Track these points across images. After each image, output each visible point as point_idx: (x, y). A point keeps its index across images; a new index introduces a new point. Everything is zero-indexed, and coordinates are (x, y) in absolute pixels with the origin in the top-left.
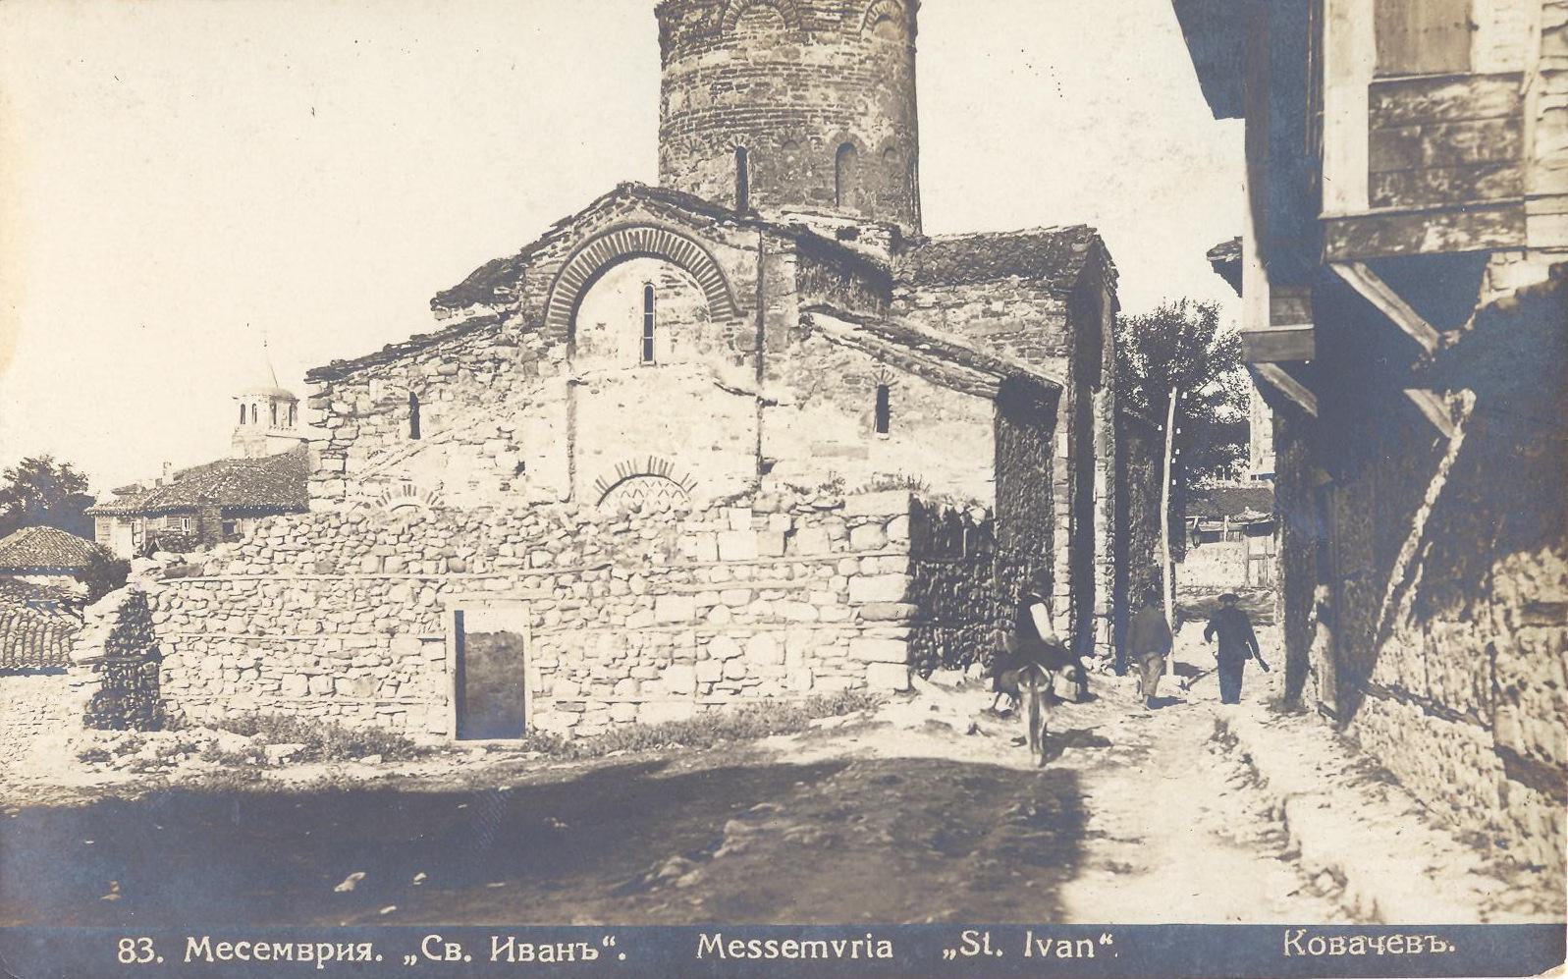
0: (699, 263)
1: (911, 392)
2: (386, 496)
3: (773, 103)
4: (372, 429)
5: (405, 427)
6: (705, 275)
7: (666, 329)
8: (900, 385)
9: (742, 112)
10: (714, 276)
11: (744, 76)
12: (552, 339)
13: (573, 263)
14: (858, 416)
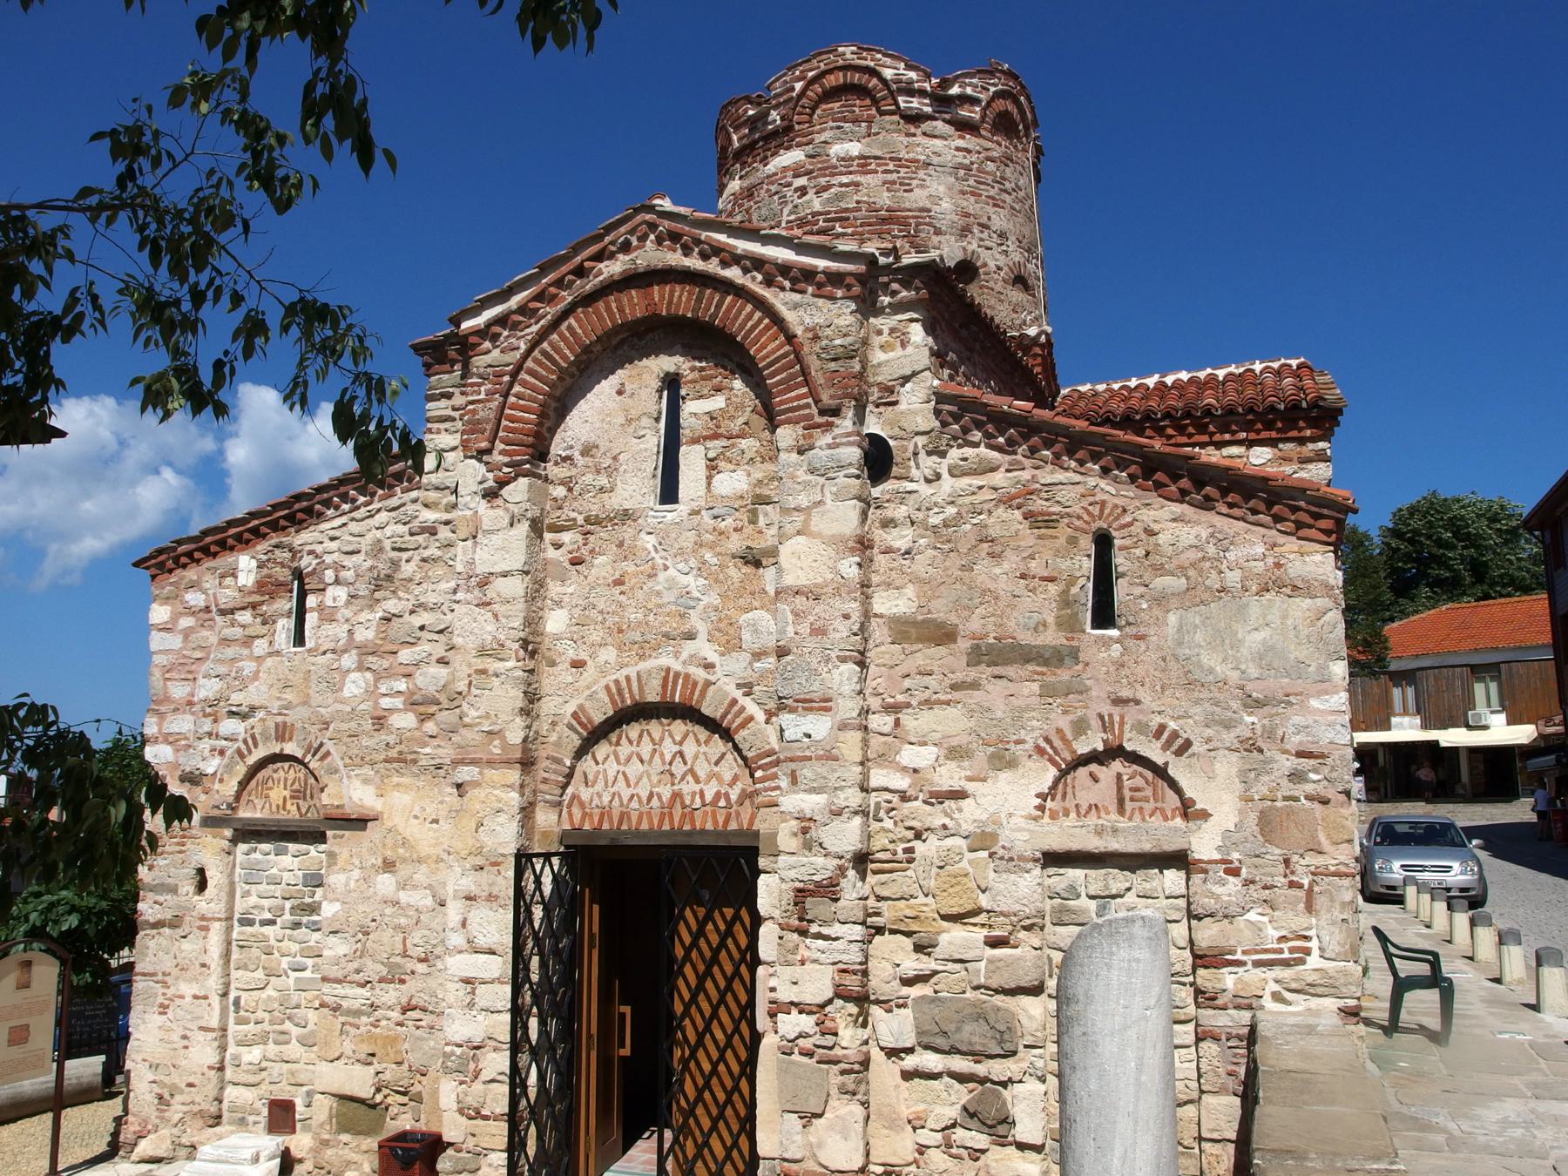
1: (1162, 539)
2: (250, 742)
4: (237, 632)
5: (285, 626)
7: (699, 448)
8: (1137, 529)
11: (825, 176)
12: (506, 470)
14: (1053, 589)
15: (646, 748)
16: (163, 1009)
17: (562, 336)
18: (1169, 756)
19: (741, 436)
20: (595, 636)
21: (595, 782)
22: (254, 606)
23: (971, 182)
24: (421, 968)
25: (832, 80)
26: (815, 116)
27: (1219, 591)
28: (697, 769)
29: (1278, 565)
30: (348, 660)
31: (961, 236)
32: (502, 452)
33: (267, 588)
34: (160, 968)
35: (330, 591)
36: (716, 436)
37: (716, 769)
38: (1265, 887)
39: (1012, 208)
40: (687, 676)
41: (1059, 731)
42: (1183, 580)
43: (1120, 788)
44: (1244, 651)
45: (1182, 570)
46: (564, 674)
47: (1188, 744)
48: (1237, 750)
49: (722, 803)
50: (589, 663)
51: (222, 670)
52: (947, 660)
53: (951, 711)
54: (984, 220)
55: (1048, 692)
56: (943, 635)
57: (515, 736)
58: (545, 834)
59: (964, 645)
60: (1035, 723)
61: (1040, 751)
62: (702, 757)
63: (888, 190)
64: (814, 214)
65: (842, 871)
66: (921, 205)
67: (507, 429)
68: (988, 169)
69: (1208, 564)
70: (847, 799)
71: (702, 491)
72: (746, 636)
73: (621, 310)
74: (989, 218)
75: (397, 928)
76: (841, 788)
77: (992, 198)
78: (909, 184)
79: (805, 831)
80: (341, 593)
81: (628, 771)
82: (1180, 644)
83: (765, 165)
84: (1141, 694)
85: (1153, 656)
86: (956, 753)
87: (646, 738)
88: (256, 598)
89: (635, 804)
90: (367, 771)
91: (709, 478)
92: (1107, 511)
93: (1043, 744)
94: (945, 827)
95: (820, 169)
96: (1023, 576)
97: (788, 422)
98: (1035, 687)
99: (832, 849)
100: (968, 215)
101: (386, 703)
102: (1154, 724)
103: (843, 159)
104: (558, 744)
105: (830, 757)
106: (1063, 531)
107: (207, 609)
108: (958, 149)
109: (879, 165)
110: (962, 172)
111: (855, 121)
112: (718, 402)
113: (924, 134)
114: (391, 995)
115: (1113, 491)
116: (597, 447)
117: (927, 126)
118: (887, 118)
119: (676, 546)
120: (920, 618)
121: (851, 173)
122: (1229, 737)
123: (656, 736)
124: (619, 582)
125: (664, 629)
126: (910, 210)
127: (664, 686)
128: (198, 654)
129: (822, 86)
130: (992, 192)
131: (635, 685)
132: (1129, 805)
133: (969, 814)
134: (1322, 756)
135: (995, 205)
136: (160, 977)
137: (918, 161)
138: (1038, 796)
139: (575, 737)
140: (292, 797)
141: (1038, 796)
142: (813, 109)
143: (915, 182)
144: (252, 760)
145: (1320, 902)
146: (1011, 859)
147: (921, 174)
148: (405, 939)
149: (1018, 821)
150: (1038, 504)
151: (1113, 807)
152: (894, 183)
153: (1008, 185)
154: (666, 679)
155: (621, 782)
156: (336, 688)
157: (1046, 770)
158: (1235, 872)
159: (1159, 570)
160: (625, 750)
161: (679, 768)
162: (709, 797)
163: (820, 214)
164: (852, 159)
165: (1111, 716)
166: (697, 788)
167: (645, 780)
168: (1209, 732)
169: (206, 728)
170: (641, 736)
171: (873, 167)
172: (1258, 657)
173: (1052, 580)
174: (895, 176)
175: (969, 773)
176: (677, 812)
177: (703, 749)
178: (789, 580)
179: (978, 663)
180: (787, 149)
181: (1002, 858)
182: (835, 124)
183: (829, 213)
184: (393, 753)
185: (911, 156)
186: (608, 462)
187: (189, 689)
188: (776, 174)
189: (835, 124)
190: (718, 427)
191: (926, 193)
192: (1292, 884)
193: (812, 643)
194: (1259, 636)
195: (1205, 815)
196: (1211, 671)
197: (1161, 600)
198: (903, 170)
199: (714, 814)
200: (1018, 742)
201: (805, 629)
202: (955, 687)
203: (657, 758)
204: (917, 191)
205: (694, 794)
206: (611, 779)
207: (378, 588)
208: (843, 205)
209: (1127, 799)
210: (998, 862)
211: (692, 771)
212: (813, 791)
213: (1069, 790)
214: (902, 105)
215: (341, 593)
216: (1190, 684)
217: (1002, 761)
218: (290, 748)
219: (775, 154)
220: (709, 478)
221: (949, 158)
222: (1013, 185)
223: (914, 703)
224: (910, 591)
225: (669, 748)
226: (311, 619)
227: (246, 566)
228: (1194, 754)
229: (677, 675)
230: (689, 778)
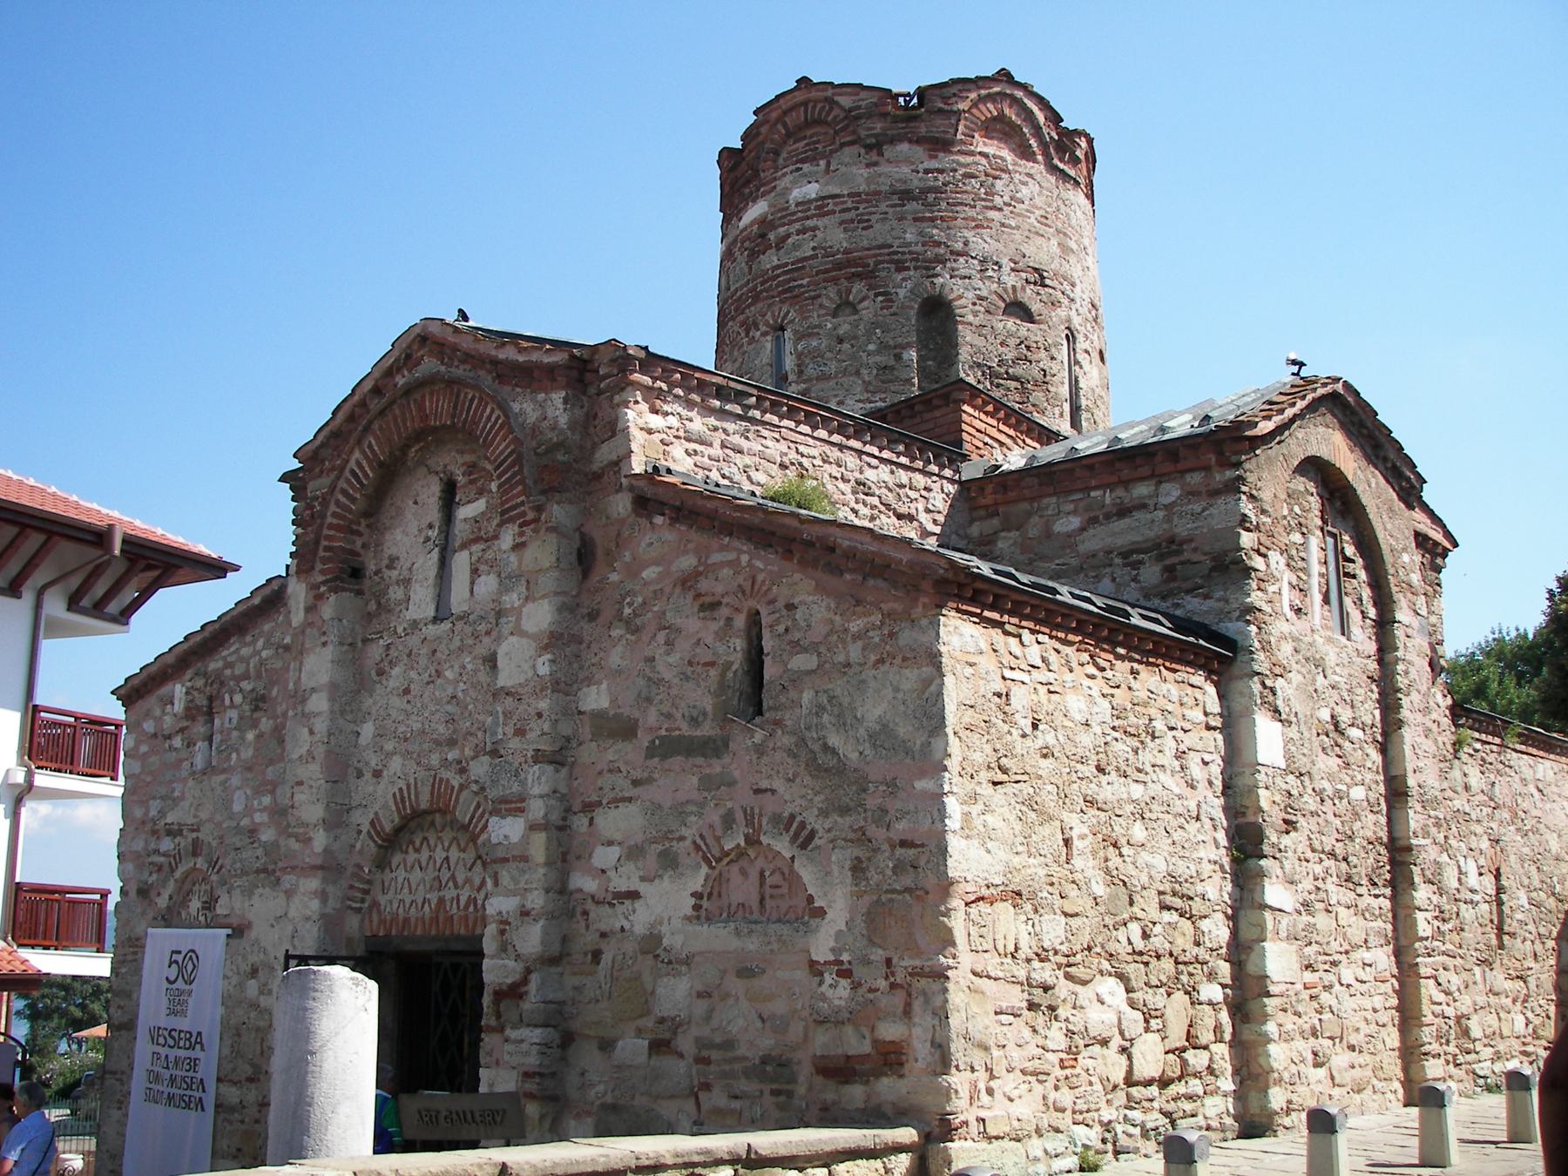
0: (492, 428)
3: (820, 252)
6: (499, 444)
9: (779, 276)
10: (507, 447)
11: (784, 225)
12: (323, 589)
13: (352, 464)
14: (713, 672)
15: (425, 855)
17: (363, 452)
18: (796, 852)
20: (389, 746)
21: (389, 889)
22: (182, 730)
23: (943, 205)
25: (791, 120)
26: (781, 161)
27: (844, 667)
28: (457, 874)
29: (892, 635)
30: (235, 780)
31: (927, 268)
32: (322, 572)
33: (191, 713)
36: (476, 540)
37: (469, 874)
38: (871, 990)
39: (1003, 225)
40: (448, 780)
41: (711, 826)
42: (815, 657)
43: (762, 883)
44: (862, 731)
45: (814, 648)
46: (366, 785)
47: (812, 834)
48: (852, 841)
49: (471, 909)
50: (385, 773)
51: (163, 791)
52: (627, 754)
53: (633, 809)
54: (959, 246)
55: (708, 784)
56: (624, 729)
57: (320, 840)
58: (350, 941)
59: (644, 739)
60: (693, 819)
61: (698, 848)
62: (461, 863)
63: (846, 230)
65: (528, 971)
66: (880, 241)
67: (327, 549)
68: (969, 188)
69: (835, 637)
70: (533, 901)
71: (468, 594)
73: (405, 424)
74: (966, 244)
75: (258, 1029)
76: (531, 890)
77: (974, 220)
78: (869, 220)
79: (503, 932)
80: (234, 714)
81: (412, 878)
82: (808, 728)
83: (740, 219)
84: (778, 784)
85: (786, 740)
86: (634, 853)
87: (425, 844)
88: (185, 724)
89: (413, 909)
91: (472, 583)
92: (756, 587)
93: (699, 841)
94: (623, 929)
95: (780, 218)
96: (690, 663)
97: (511, 520)
98: (695, 780)
99: (521, 951)
100: (938, 244)
101: (258, 818)
102: (786, 814)
103: (798, 204)
104: (361, 852)
105: (525, 859)
106: (725, 611)
107: (155, 735)
108: (927, 171)
109: (836, 204)
110: (931, 197)
111: (812, 160)
112: (480, 506)
113: (888, 161)
114: (251, 1096)
115: (764, 563)
116: (398, 558)
117: (889, 151)
118: (847, 150)
119: (447, 652)
120: (612, 713)
121: (808, 218)
122: (845, 822)
123: (432, 843)
124: (407, 691)
125: (435, 736)
126: (868, 249)
127: (432, 794)
128: (149, 779)
129: (785, 125)
130: (971, 213)
131: (413, 792)
132: (769, 903)
133: (640, 918)
134: (922, 845)
135: (977, 227)
136: (118, 1076)
137: (878, 193)
138: (692, 895)
139: (372, 844)
140: (203, 908)
141: (692, 895)
142: (777, 153)
143: (874, 218)
144: (178, 874)
145: (917, 1005)
146: (670, 962)
147: (883, 207)
148: (263, 1040)
149: (677, 923)
150: (704, 585)
151: (755, 905)
152: (852, 221)
153: (998, 201)
154: (433, 785)
155: (406, 891)
156: (227, 803)
157: (698, 866)
158: (845, 973)
159: (797, 647)
160: (412, 857)
161: (445, 875)
162: (462, 903)
163: (778, 267)
164: (810, 201)
165: (752, 808)
166: (454, 893)
167: (421, 887)
169: (153, 846)
170: (422, 844)
171: (830, 207)
172: (872, 736)
173: (712, 664)
174: (852, 214)
175: (641, 873)
176: (441, 919)
177: (462, 855)
178: (505, 679)
179: (652, 757)
180: (754, 201)
181: (663, 962)
182: (794, 167)
183: (786, 264)
185: (872, 187)
186: (405, 573)
187: (143, 810)
188: (745, 229)
189: (794, 167)
190: (480, 529)
191: (887, 227)
192: (893, 986)
193: (514, 744)
194: (878, 712)
195: (821, 913)
196: (834, 752)
197: (797, 679)
198: (862, 206)
199: (467, 916)
200: (682, 838)
201: (510, 730)
202: (636, 783)
203: (431, 865)
204: (878, 226)
205: (453, 899)
206: (399, 886)
207: (257, 709)
208: (798, 254)
209: (767, 897)
210: (660, 965)
211: (453, 877)
212: (510, 893)
213: (724, 891)
214: (863, 133)
215: (234, 714)
217: (669, 861)
219: (745, 209)
220: (472, 583)
221: (916, 183)
222: (1006, 199)
223: (604, 802)
224: (604, 686)
225: (440, 855)
226: (217, 738)
227: (179, 690)
228: (818, 847)
229: (441, 779)
230: (451, 884)
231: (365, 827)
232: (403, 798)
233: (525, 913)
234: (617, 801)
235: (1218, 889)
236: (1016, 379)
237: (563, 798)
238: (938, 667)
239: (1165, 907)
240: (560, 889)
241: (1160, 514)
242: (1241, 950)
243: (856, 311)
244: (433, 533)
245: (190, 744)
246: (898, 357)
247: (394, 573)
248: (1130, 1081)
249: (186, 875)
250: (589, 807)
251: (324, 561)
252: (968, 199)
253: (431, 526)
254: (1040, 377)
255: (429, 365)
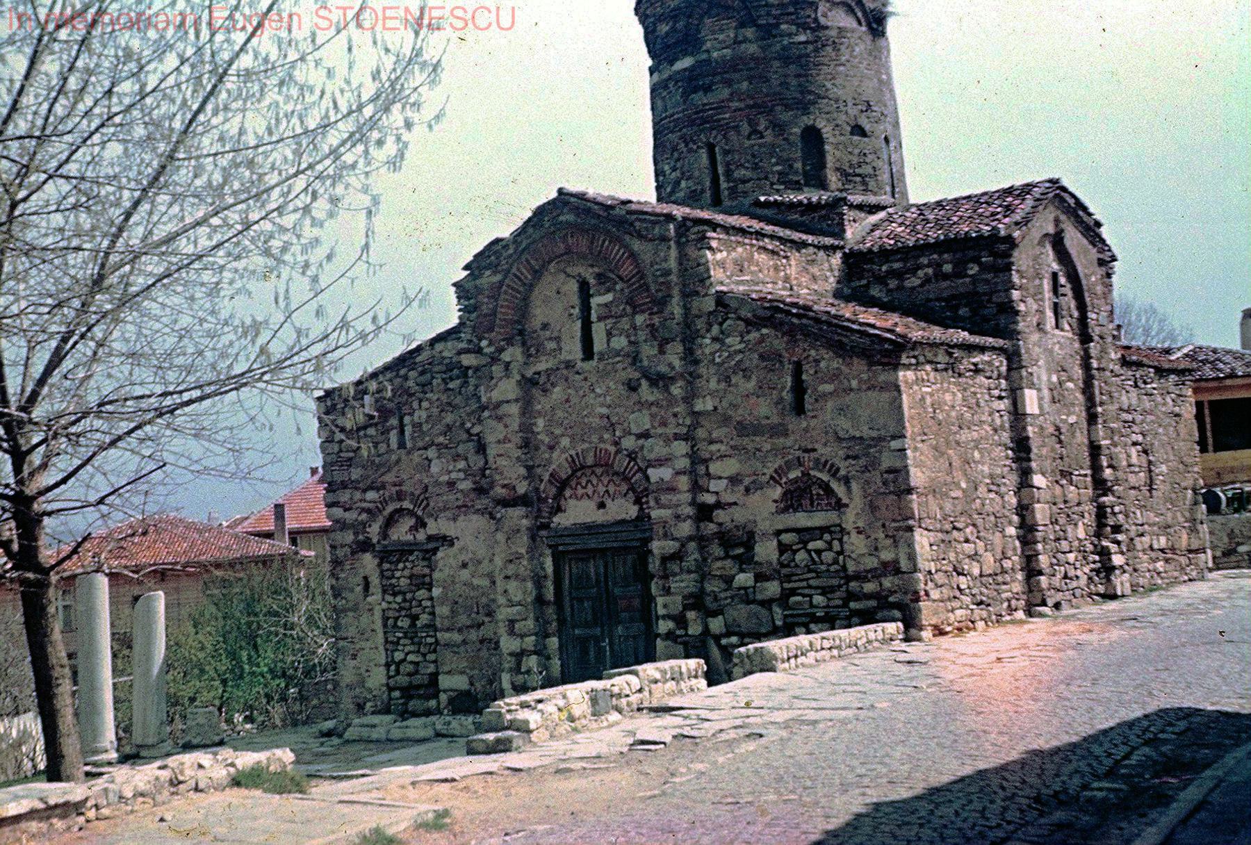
7: (602, 324)
15: (590, 490)
16: (354, 657)
19: (622, 316)
24: (487, 619)
30: (431, 453)
34: (350, 635)
35: (416, 414)
47: (838, 469)
53: (733, 461)
64: (704, 105)
72: (632, 426)
80: (424, 415)
90: (449, 514)
91: (608, 341)
101: (454, 475)
102: (823, 460)
112: (609, 297)
114: (473, 635)
123: (595, 482)
124: (567, 401)
168: (847, 463)
184: (460, 503)
186: (556, 334)
216: (840, 439)
218: (407, 504)
225: (601, 489)
231: (546, 477)
232: (573, 461)
233: (678, 517)
234: (722, 457)
235: (1012, 480)
236: (859, 175)
237: (690, 457)
238: (899, 391)
239: (990, 491)
240: (693, 503)
241: (967, 280)
242: (1023, 510)
243: (762, 137)
244: (576, 311)
245: (386, 432)
246: (791, 166)
247: (548, 333)
248: (981, 576)
249: (392, 515)
250: (705, 461)
251: (502, 327)
252: (826, 60)
253: (573, 307)
254: (872, 172)
255: (568, 217)
